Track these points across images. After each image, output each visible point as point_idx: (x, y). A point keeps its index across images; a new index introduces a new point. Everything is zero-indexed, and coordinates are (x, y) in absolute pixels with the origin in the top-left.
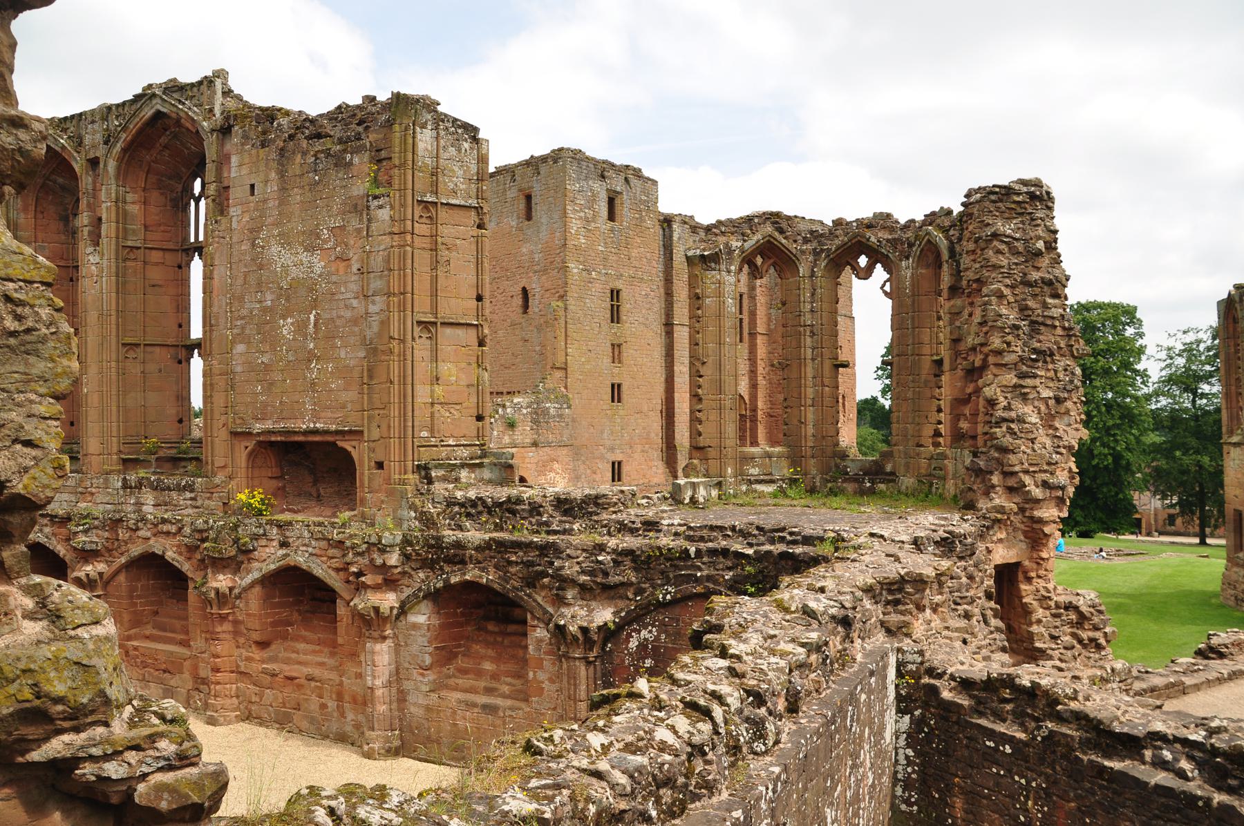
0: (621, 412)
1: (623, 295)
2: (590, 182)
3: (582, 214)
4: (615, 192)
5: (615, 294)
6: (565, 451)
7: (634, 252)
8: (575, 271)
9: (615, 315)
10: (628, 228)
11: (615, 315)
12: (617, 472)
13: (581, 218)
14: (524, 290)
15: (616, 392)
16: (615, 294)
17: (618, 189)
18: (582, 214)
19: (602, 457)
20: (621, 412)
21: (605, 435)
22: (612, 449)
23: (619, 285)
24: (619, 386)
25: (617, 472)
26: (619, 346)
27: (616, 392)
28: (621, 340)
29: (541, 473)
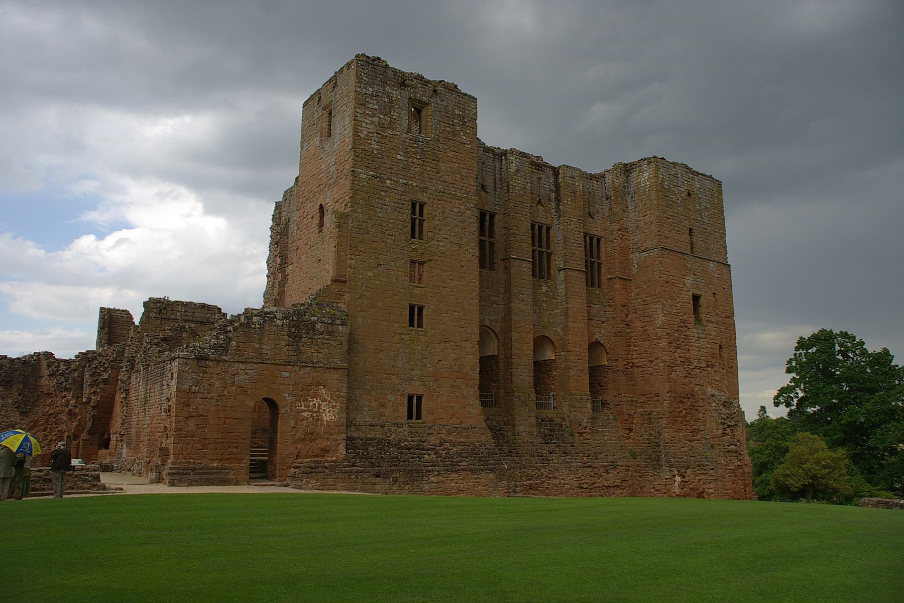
3: (376, 119)
4: (421, 102)
5: (417, 208)
6: (336, 375)
7: (443, 166)
8: (364, 176)
9: (416, 230)
11: (416, 230)
12: (414, 406)
13: (372, 123)
14: (321, 206)
15: (415, 315)
16: (417, 208)
23: (422, 197)
24: (421, 309)
25: (414, 406)
26: (422, 264)
27: (415, 315)
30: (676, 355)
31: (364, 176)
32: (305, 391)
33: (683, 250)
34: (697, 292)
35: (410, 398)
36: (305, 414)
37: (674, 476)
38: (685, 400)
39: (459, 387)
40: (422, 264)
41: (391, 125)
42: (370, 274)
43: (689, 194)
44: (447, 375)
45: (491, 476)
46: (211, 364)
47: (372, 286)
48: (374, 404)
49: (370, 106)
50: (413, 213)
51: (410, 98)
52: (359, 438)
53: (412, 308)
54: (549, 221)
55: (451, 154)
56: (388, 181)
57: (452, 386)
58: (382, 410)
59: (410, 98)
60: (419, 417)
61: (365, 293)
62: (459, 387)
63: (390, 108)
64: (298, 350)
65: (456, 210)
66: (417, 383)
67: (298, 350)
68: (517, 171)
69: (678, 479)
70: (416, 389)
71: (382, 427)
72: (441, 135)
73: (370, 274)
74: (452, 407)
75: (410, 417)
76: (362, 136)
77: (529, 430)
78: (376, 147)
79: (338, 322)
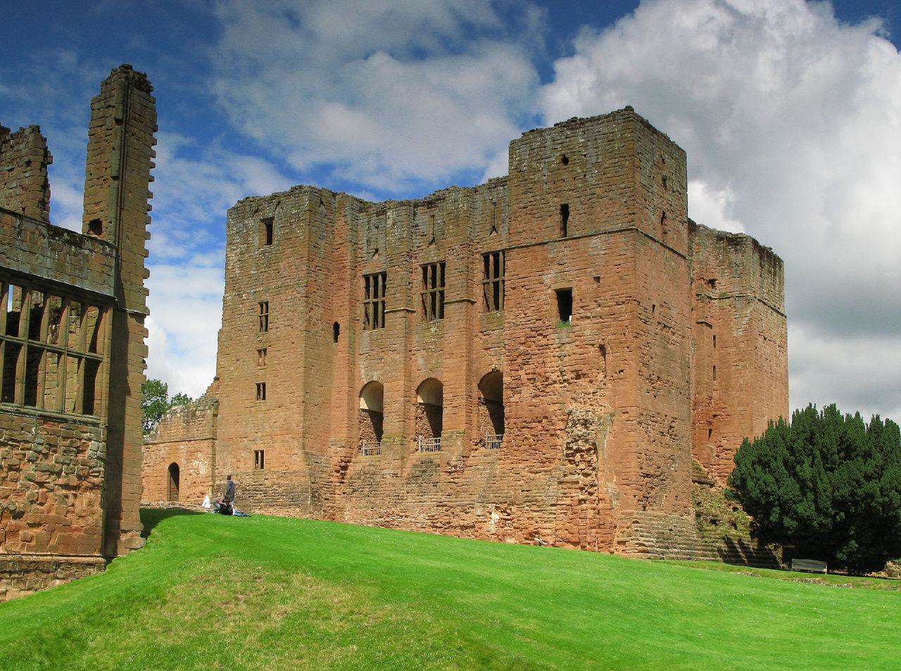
4: (268, 219)
12: (259, 457)
15: (261, 390)
16: (264, 305)
23: (265, 298)
27: (261, 390)
29: (189, 461)
30: (521, 373)
31: (229, 298)
32: (192, 454)
34: (559, 286)
36: (191, 471)
37: (490, 513)
38: (534, 425)
39: (287, 441)
40: (265, 350)
43: (565, 161)
44: (278, 433)
45: (298, 510)
46: (151, 446)
51: (261, 220)
53: (258, 386)
54: (441, 258)
62: (287, 441)
64: (188, 431)
67: (188, 431)
68: (394, 224)
69: (496, 516)
70: (260, 448)
74: (282, 457)
77: (392, 472)
79: (207, 408)
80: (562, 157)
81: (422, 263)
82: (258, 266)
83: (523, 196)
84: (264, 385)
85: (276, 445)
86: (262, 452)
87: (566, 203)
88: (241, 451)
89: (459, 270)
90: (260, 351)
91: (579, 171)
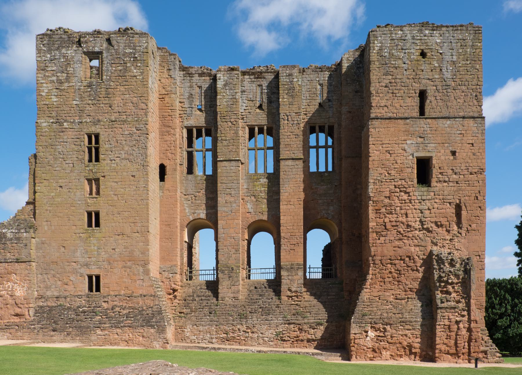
0: (98, 235)
1: (102, 138)
2: (64, 51)
3: (54, 78)
8: (45, 124)
9: (94, 154)
10: (110, 80)
11: (94, 154)
12: (95, 283)
15: (94, 219)
16: (94, 139)
17: (97, 49)
18: (54, 78)
19: (75, 272)
20: (98, 235)
21: (78, 254)
22: (87, 265)
23: (94, 129)
25: (95, 283)
27: (94, 219)
28: (98, 175)
31: (45, 124)
33: (406, 115)
35: (90, 277)
41: (68, 79)
42: (53, 194)
43: (423, 54)
47: (55, 203)
48: (59, 283)
49: (49, 69)
50: (90, 142)
52: (48, 306)
53: (89, 214)
55: (122, 89)
56: (65, 124)
57: (125, 267)
58: (66, 286)
59: (85, 53)
60: (98, 289)
61: (49, 208)
63: (66, 66)
65: (127, 133)
66: (93, 267)
70: (95, 271)
71: (65, 298)
72: (113, 75)
73: (53, 194)
75: (90, 289)
76: (44, 94)
78: (55, 100)
80: (420, 51)
81: (250, 124)
82: (82, 98)
83: (384, 77)
84: (97, 214)
85: (115, 271)
86: (98, 278)
87: (425, 88)
88: (69, 274)
89: (294, 133)
90: (89, 181)
91: (436, 65)
